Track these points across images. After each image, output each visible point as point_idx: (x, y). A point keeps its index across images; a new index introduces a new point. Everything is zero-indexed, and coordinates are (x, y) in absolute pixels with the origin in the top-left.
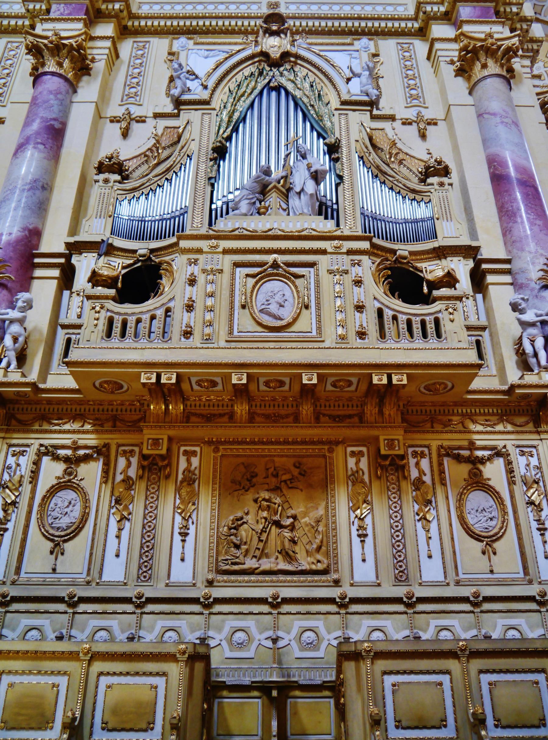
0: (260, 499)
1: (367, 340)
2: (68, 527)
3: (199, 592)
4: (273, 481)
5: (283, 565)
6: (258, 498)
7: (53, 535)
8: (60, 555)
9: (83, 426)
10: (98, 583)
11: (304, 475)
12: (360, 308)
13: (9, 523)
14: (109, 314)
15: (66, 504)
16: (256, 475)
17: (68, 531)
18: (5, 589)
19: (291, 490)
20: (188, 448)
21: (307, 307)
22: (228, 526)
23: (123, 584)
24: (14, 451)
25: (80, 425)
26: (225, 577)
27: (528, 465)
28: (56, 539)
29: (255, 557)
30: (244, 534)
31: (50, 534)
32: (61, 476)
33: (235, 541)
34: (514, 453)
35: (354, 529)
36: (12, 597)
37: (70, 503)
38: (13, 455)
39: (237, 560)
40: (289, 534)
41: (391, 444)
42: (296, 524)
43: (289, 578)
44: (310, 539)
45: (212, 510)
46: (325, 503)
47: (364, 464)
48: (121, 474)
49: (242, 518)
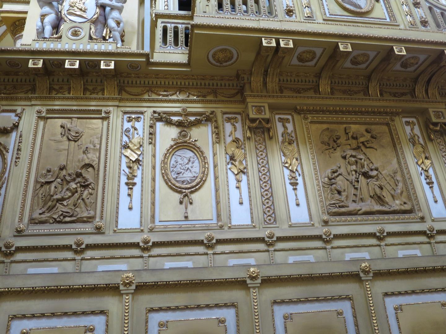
1: (428, 28)
2: (192, 181)
3: (319, 230)
4: (354, 143)
5: (378, 208)
6: (346, 155)
7: (180, 188)
8: (189, 205)
9: (188, 97)
10: (230, 227)
11: (375, 138)
13: (135, 178)
15: (187, 161)
17: (194, 184)
18: (146, 236)
20: (282, 116)
22: (328, 177)
23: (252, 227)
24: (129, 117)
25: (186, 96)
26: (338, 218)
28: (184, 191)
31: (176, 187)
32: (177, 139)
35: (423, 178)
36: (154, 243)
37: (189, 161)
38: (129, 121)
39: (343, 204)
43: (386, 217)
45: (314, 164)
46: (396, 159)
47: (417, 130)
48: (229, 136)
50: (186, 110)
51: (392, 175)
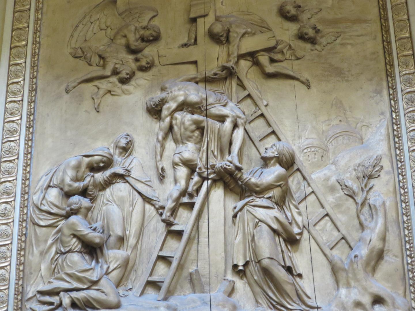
0: (173, 105)
6: (163, 102)
11: (313, 41)
16: (156, 39)
19: (273, 83)
29: (155, 285)
30: (115, 211)
33: (84, 229)
39: (93, 293)
40: (275, 212)
42: (294, 182)
44: (344, 232)
46: (385, 121)
49: (108, 163)
51: (349, 183)
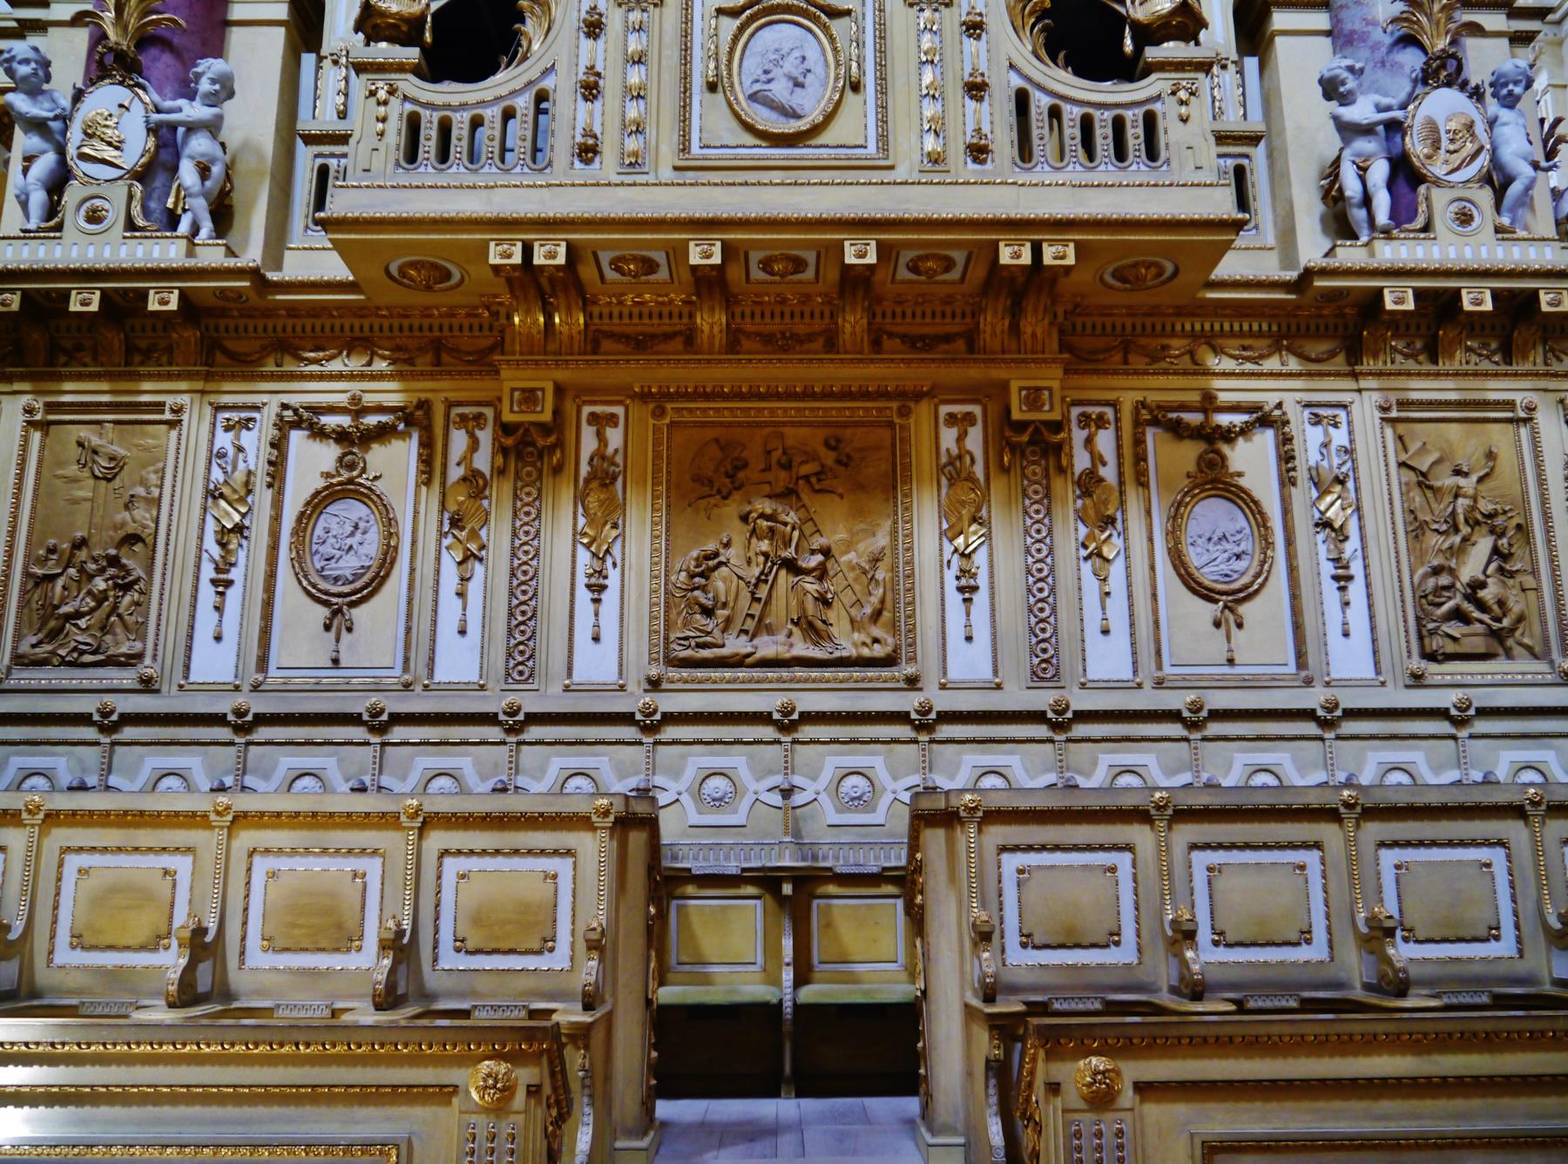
0: (754, 515)
1: (989, 166)
2: (357, 577)
3: (634, 701)
4: (782, 478)
5: (802, 649)
6: (750, 513)
7: (326, 593)
8: (344, 632)
9: (369, 364)
10: (426, 686)
11: (846, 465)
12: (976, 89)
13: (233, 569)
14: (409, 107)
15: (349, 529)
16: (745, 465)
17: (358, 584)
18: (240, 700)
19: (819, 496)
20: (598, 409)
21: (856, 87)
22: (687, 570)
24: (228, 420)
25: (365, 360)
26: (685, 673)
27: (1325, 445)
28: (334, 600)
29: (746, 632)
30: (720, 585)
31: (319, 590)
32: (334, 473)
33: (703, 600)
34: (1298, 419)
35: (950, 576)
36: (256, 715)
37: (356, 527)
38: (227, 429)
39: (708, 639)
40: (816, 587)
41: (1033, 398)
42: (829, 565)
43: (815, 673)
44: (859, 596)
45: (654, 537)
46: (889, 522)
47: (975, 440)
48: (458, 464)
49: (716, 554)
50: (360, 399)
51: (863, 564)
